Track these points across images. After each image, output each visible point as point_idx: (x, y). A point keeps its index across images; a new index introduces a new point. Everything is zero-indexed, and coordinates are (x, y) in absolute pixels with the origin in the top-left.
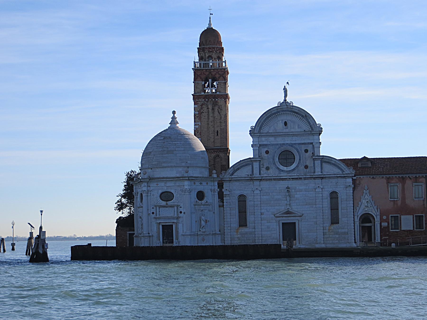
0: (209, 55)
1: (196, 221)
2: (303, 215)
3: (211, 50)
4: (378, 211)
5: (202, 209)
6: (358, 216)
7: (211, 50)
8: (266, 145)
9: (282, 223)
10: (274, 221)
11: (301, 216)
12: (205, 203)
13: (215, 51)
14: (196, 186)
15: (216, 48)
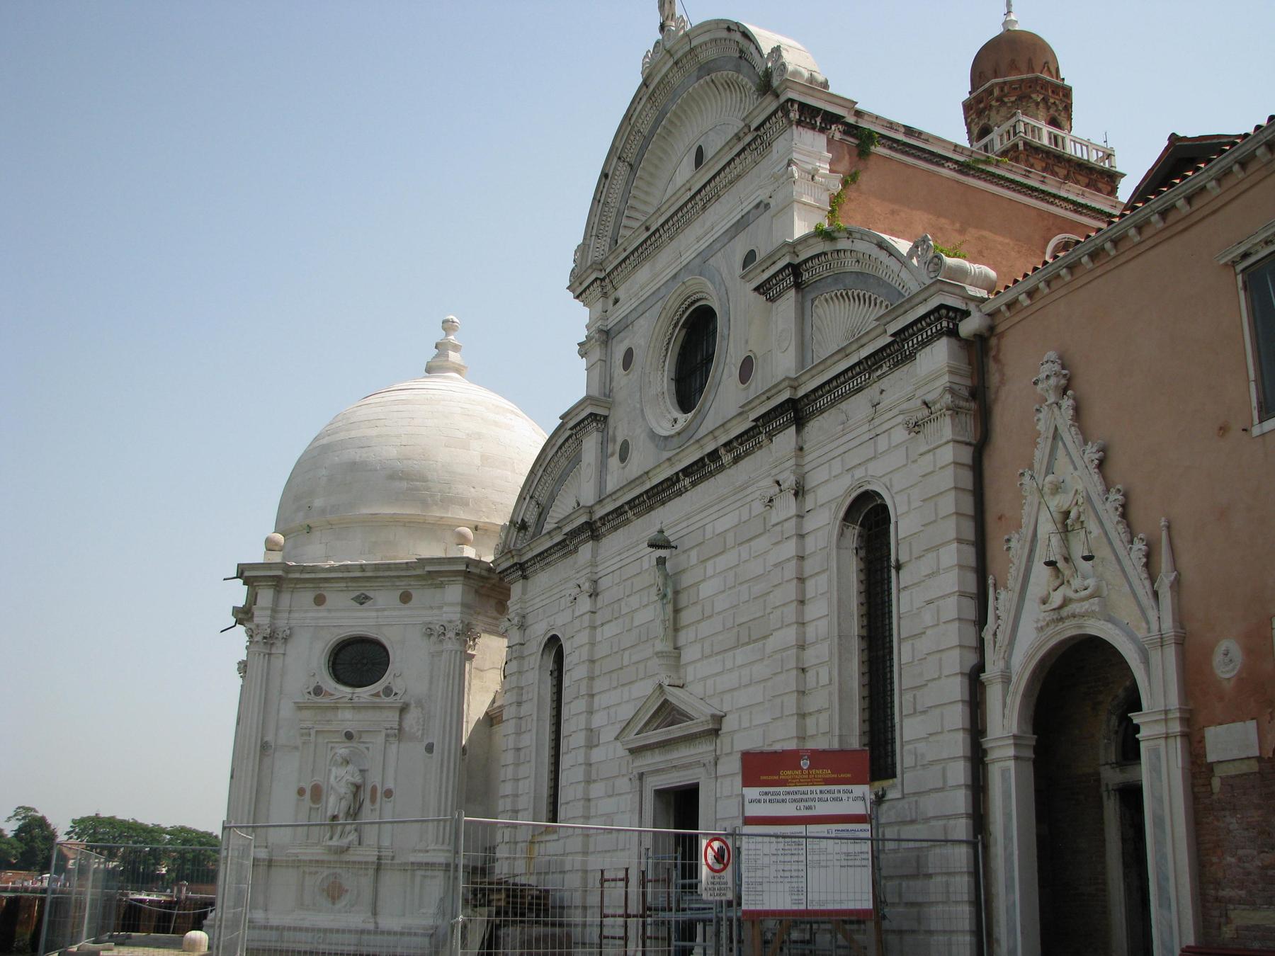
0: (981, 123)
1: (301, 792)
2: (727, 726)
3: (982, 106)
4: (1156, 594)
5: (349, 727)
6: (1006, 679)
7: (982, 106)
8: (625, 325)
9: (660, 793)
10: (623, 784)
11: (715, 732)
12: (377, 695)
13: (994, 103)
14: (325, 614)
15: (1002, 90)
